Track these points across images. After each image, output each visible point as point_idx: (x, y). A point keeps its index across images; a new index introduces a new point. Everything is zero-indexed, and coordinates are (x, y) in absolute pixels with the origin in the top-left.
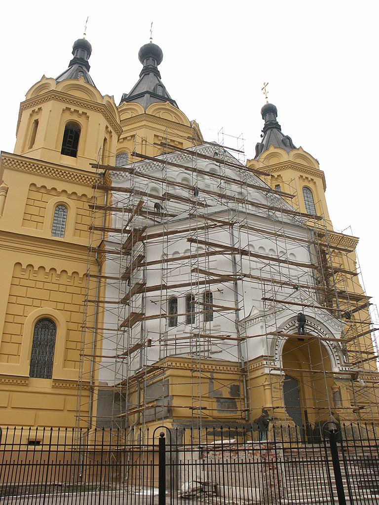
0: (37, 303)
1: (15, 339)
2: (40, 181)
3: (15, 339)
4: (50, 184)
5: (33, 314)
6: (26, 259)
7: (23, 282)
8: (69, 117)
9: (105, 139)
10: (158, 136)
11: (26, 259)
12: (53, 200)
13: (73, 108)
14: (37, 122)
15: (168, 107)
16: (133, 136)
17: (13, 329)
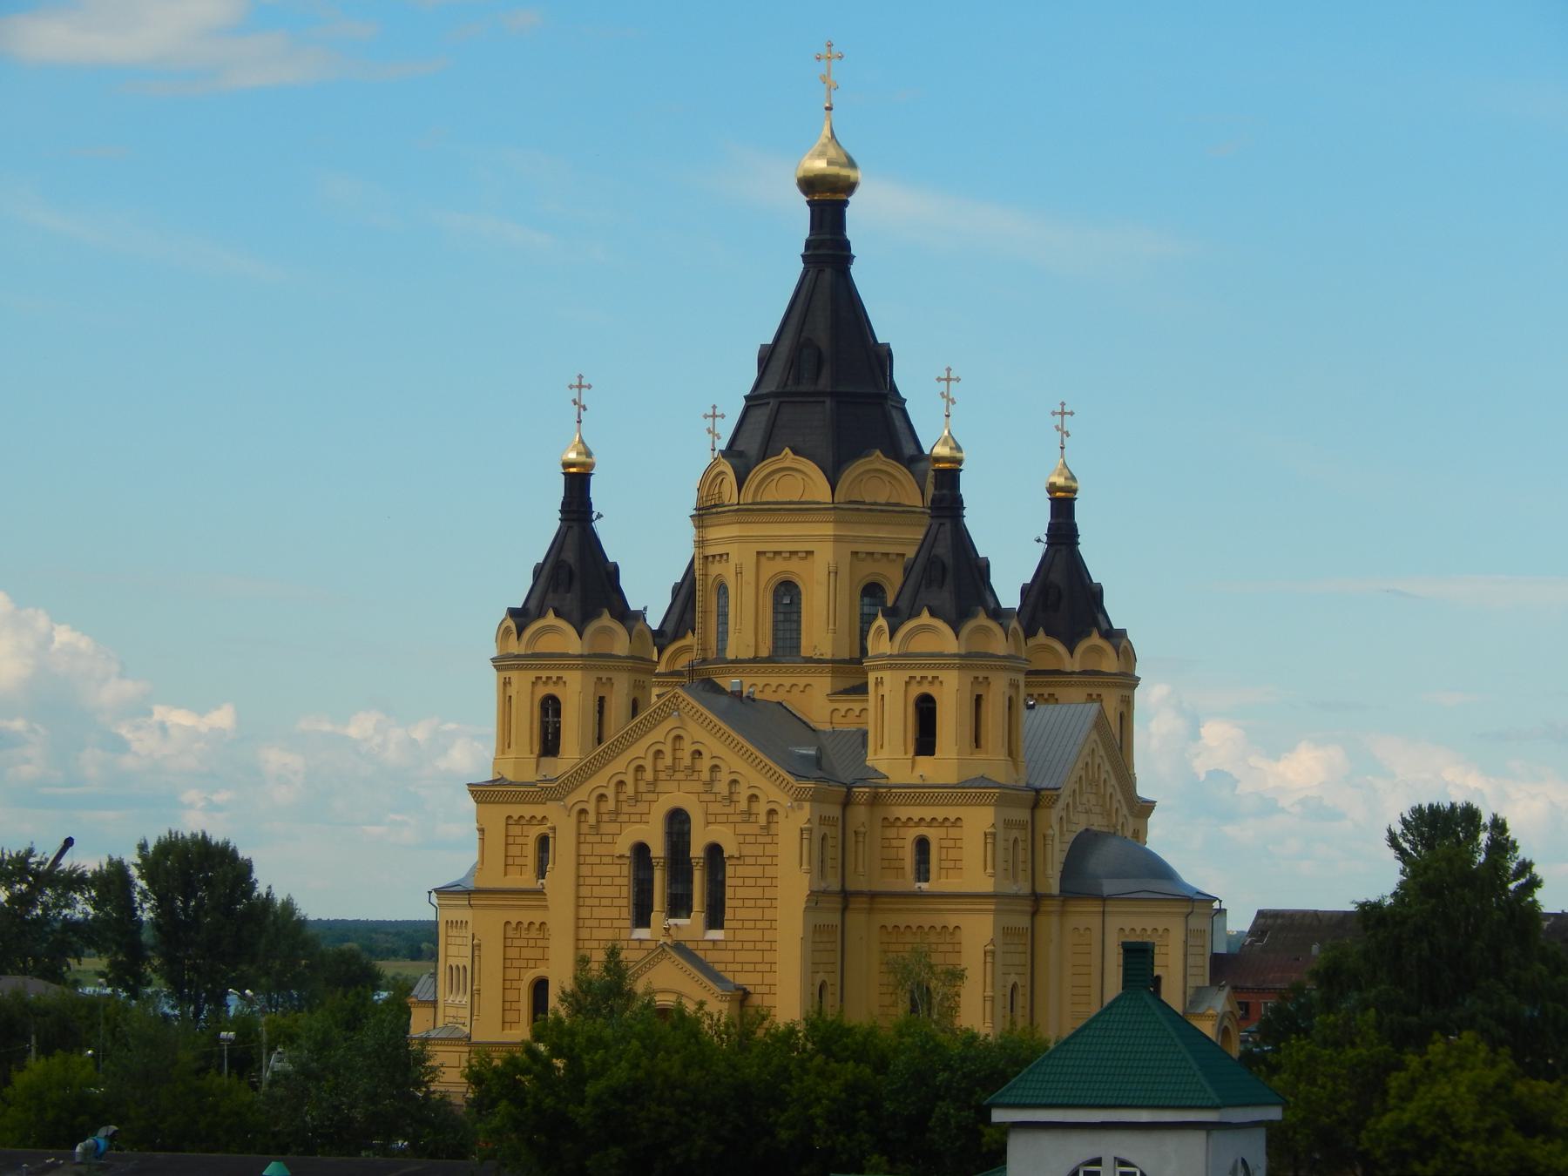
0: (531, 964)
1: (515, 1006)
2: (517, 810)
3: (515, 1006)
4: (527, 811)
5: (529, 976)
6: (514, 916)
7: (516, 943)
8: (543, 691)
9: (602, 699)
10: (765, 553)
11: (514, 916)
12: (535, 832)
13: (544, 674)
14: (510, 697)
15: (787, 464)
16: (728, 554)
17: (511, 995)
